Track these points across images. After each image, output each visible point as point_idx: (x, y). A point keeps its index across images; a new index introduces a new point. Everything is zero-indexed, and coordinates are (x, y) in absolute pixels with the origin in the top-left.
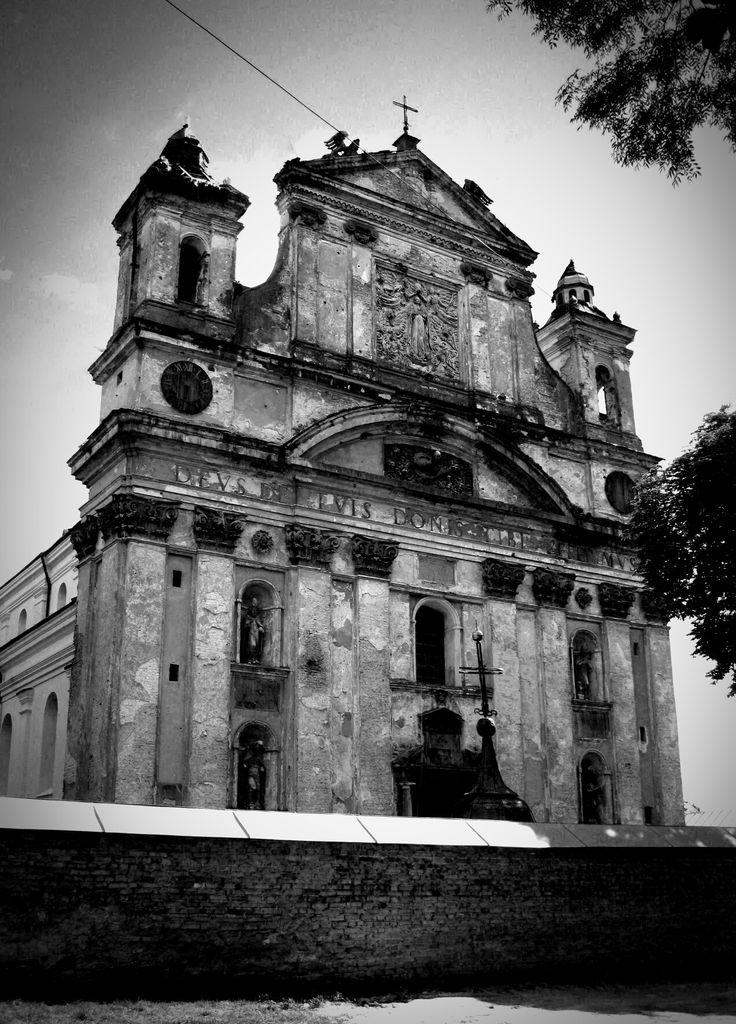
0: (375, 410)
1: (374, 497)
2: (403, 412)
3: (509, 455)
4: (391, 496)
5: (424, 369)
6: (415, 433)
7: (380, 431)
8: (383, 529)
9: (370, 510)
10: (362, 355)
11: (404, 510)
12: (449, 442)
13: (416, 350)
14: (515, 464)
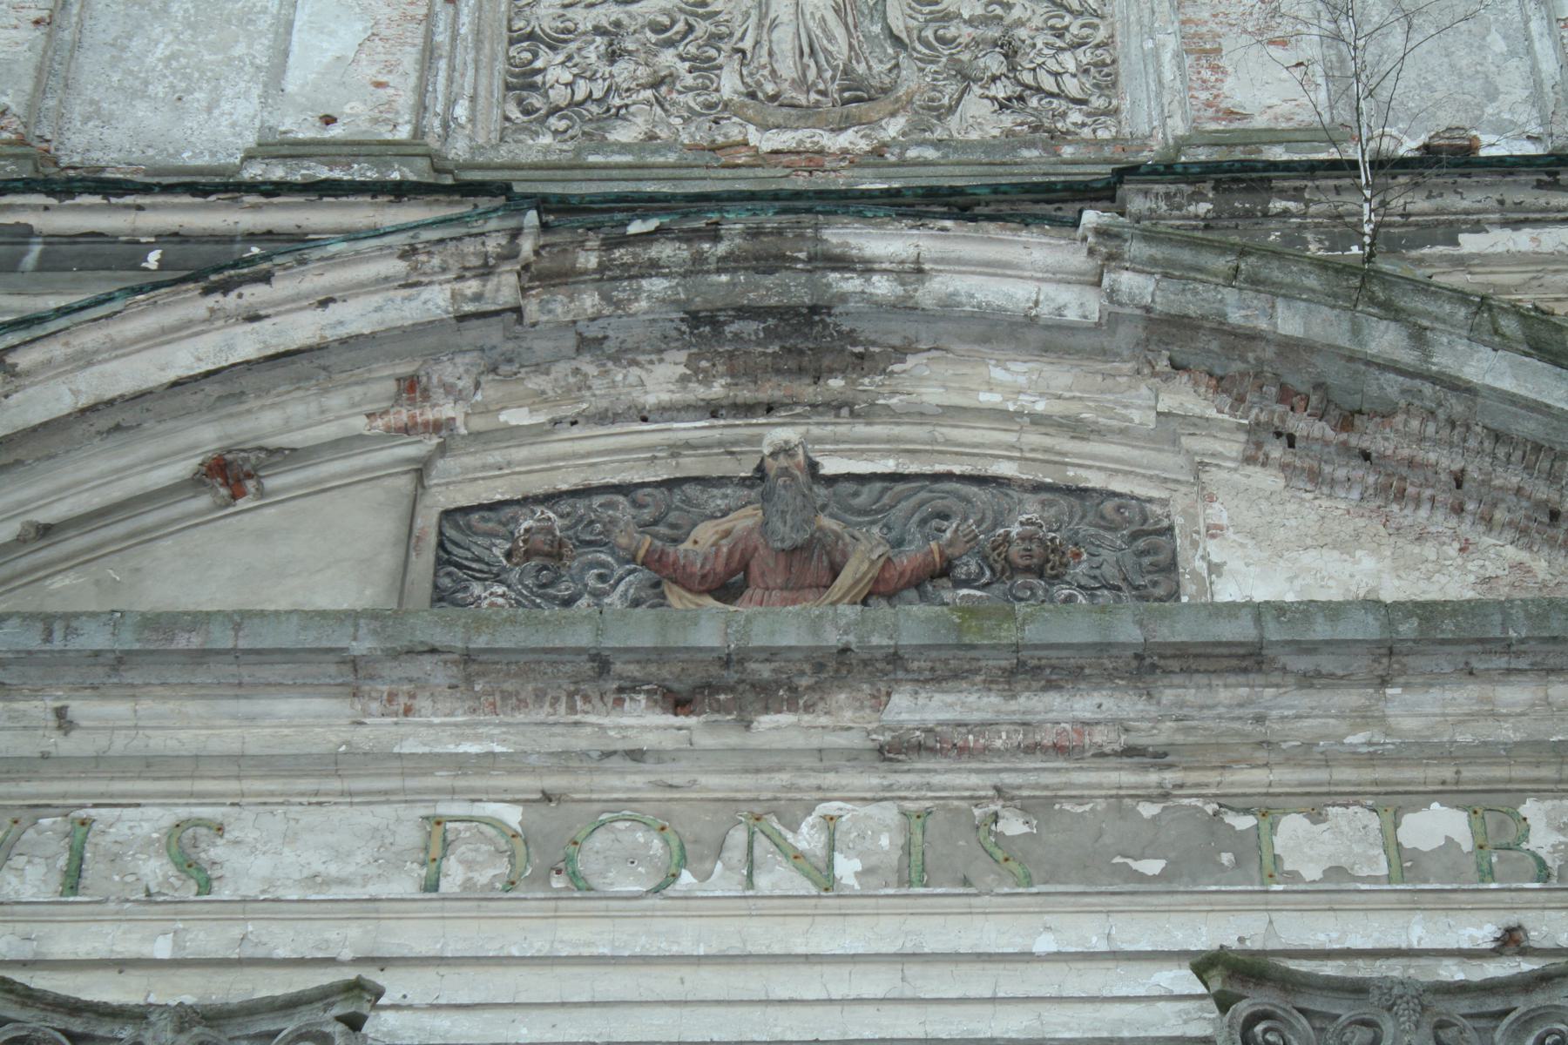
0: (254, 294)
1: (239, 763)
2: (485, 271)
3: (1385, 339)
4: (379, 730)
5: (846, 139)
6: (651, 400)
7: (359, 424)
8: (283, 940)
9: (217, 851)
10: (335, 132)
11: (512, 816)
12: (932, 395)
13: (787, 68)
14: (1466, 390)
